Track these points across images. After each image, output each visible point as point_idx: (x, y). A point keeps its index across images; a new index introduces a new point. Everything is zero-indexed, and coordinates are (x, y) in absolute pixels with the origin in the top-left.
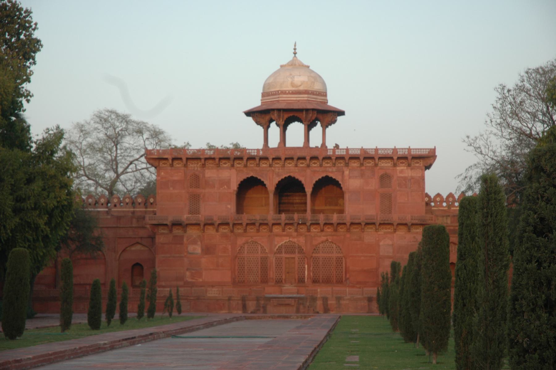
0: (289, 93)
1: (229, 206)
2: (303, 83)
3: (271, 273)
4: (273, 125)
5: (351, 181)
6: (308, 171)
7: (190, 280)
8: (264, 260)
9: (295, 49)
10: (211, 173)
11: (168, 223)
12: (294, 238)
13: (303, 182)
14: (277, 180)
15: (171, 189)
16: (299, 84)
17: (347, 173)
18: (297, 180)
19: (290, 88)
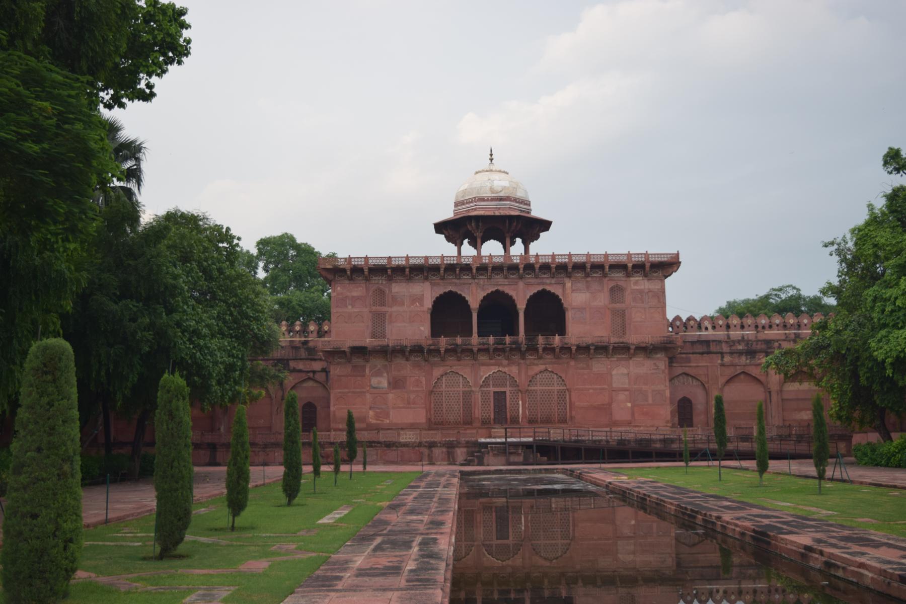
0: (488, 200)
1: (422, 328)
2: (504, 188)
3: (477, 411)
4: (466, 241)
5: (575, 296)
6: (521, 284)
7: (374, 421)
8: (467, 395)
9: (491, 155)
10: (399, 288)
11: (346, 349)
12: (504, 366)
13: (515, 297)
14: (482, 294)
15: (350, 307)
16: (500, 189)
17: (569, 284)
18: (507, 294)
19: (490, 195)
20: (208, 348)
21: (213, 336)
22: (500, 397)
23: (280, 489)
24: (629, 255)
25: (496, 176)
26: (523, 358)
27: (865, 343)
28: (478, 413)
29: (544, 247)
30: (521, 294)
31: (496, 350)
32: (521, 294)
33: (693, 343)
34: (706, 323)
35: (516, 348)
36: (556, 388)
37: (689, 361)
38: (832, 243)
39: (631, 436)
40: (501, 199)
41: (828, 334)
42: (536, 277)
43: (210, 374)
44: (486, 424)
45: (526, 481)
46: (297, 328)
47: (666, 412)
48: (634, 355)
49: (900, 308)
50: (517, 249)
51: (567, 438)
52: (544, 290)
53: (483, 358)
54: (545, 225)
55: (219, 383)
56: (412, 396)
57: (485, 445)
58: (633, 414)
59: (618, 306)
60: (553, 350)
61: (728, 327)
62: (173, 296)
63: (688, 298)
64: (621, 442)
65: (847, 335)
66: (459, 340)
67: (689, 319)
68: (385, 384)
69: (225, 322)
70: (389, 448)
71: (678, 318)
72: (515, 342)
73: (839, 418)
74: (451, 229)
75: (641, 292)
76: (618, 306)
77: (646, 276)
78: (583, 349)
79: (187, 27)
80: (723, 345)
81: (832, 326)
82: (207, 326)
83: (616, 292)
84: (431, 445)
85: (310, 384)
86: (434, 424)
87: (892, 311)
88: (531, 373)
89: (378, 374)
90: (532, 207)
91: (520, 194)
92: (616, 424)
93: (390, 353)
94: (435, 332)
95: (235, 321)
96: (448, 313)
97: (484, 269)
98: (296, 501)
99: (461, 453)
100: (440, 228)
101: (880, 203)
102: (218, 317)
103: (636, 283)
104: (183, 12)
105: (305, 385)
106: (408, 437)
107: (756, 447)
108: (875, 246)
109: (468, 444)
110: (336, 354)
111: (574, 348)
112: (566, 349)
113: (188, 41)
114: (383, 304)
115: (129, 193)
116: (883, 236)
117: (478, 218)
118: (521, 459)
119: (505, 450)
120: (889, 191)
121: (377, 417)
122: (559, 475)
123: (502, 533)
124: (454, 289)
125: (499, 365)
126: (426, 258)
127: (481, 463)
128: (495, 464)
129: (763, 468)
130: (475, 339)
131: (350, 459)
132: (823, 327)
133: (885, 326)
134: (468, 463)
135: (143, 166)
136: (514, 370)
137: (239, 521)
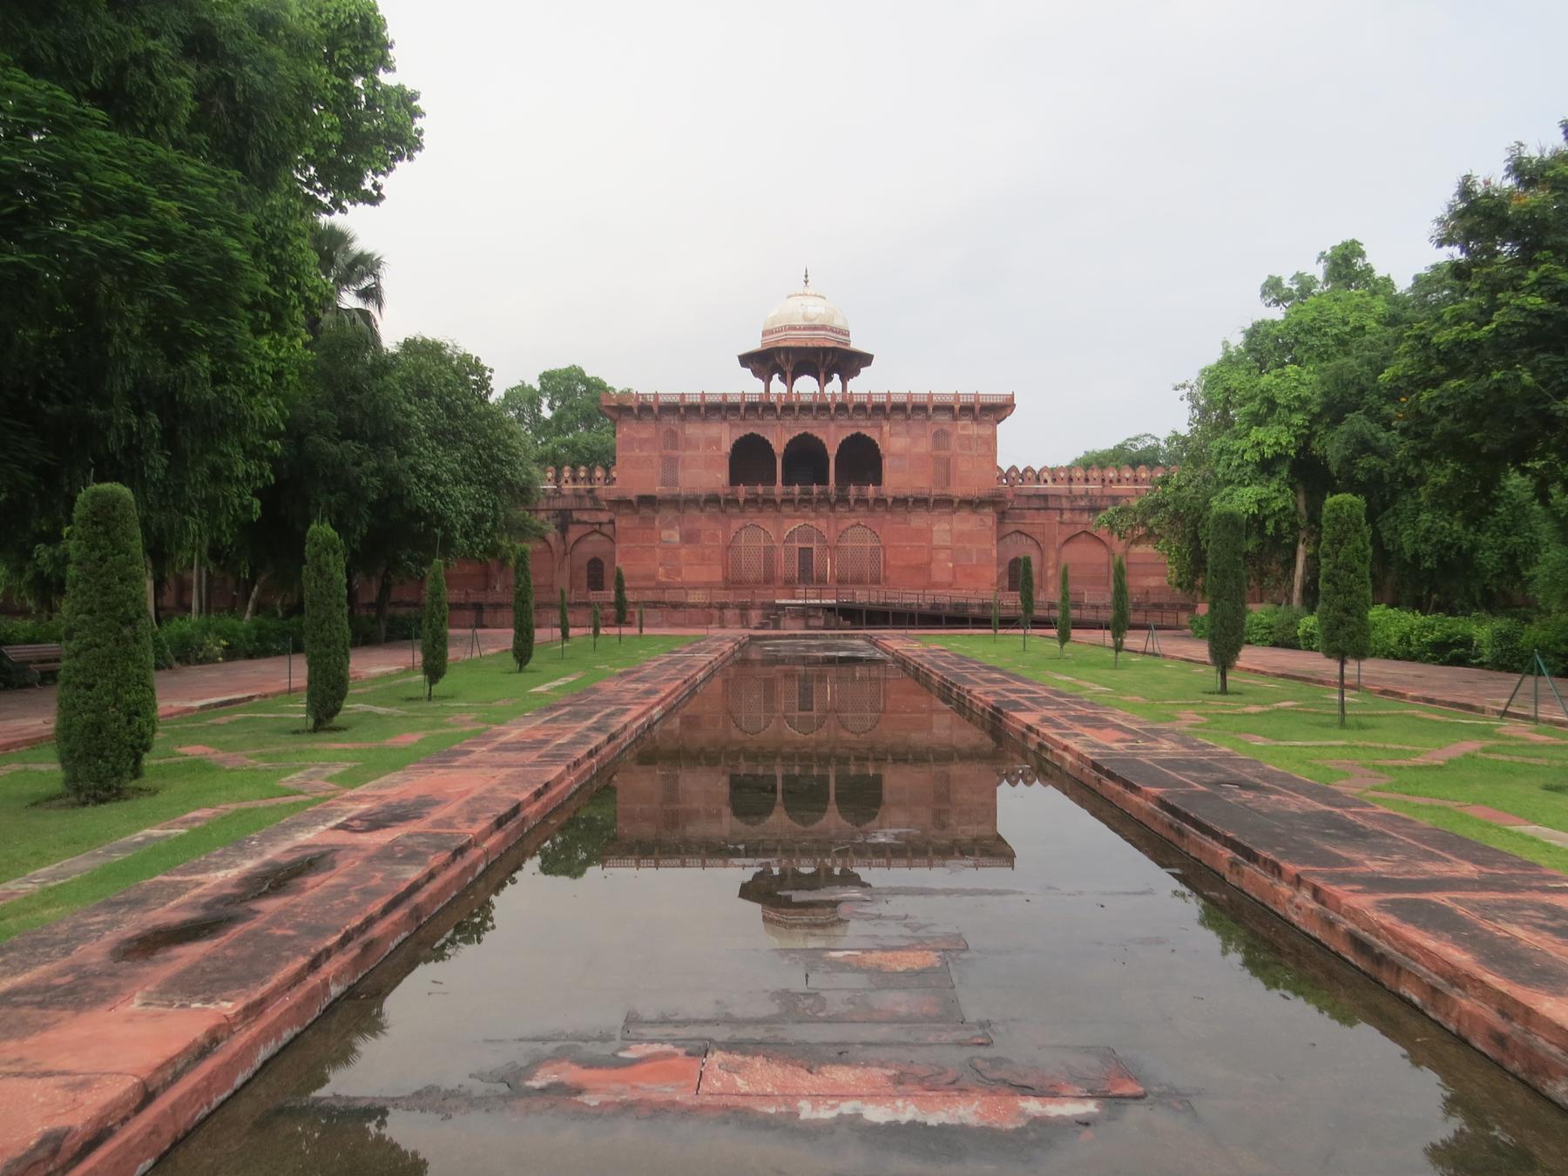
4: (776, 377)
5: (894, 442)
6: (832, 426)
8: (769, 552)
10: (694, 430)
14: (787, 438)
17: (886, 428)
19: (802, 323)
20: (450, 496)
21: (457, 482)
22: (806, 554)
23: (511, 655)
24: (957, 395)
25: (810, 301)
26: (833, 509)
27: (1207, 501)
28: (781, 571)
29: (864, 384)
30: (832, 437)
31: (801, 501)
32: (832, 437)
33: (1029, 497)
34: (1046, 475)
35: (824, 500)
36: (869, 544)
37: (1024, 517)
38: (1184, 386)
39: (945, 600)
40: (815, 328)
41: (1169, 490)
42: (850, 418)
43: (453, 526)
44: (789, 584)
45: (818, 648)
46: (582, 474)
47: (992, 573)
48: (958, 509)
49: (1248, 463)
50: (835, 385)
51: (873, 601)
52: (858, 434)
53: (787, 510)
54: (866, 359)
55: (466, 535)
56: (707, 552)
57: (783, 607)
58: (954, 576)
59: (942, 453)
60: (866, 501)
61: (1071, 480)
62: (407, 436)
63: (1028, 446)
64: (935, 606)
65: (1189, 491)
66: (760, 489)
67: (1026, 470)
68: (677, 538)
69: (472, 466)
70: (672, 609)
71: (1014, 468)
72: (825, 493)
73: (1180, 585)
74: (761, 362)
75: (969, 437)
76: (942, 453)
77: (975, 419)
78: (901, 502)
79: (421, 114)
80: (1064, 500)
81: (1174, 481)
82: (450, 471)
83: (940, 437)
84: (723, 606)
85: (596, 537)
86: (731, 583)
87: (1239, 466)
88: (842, 527)
89: (670, 526)
90: (851, 338)
91: (838, 323)
92: (935, 586)
93: (678, 503)
94: (734, 479)
95: (486, 466)
96: (749, 458)
97: (790, 409)
98: (531, 665)
99: (755, 616)
100: (746, 360)
101: (1237, 341)
102: (463, 460)
103: (963, 428)
104: (414, 96)
105: (590, 538)
106: (696, 597)
107: (1056, 614)
108: (1227, 390)
109: (763, 606)
110: (621, 503)
111: (890, 500)
112: (880, 501)
113: (420, 132)
114: (675, 447)
115: (366, 315)
116: (1236, 379)
117: (787, 350)
118: (822, 623)
119: (805, 613)
120: (1248, 326)
121: (668, 575)
122: (857, 642)
123: (806, 705)
124: (756, 431)
125: (805, 517)
126: (725, 395)
127: (776, 627)
128: (793, 628)
129: (1064, 638)
130: (779, 488)
131: (621, 620)
132: (1165, 482)
133: (1230, 482)
134: (763, 626)
135: (383, 283)
136: (822, 524)
137: (438, 688)
